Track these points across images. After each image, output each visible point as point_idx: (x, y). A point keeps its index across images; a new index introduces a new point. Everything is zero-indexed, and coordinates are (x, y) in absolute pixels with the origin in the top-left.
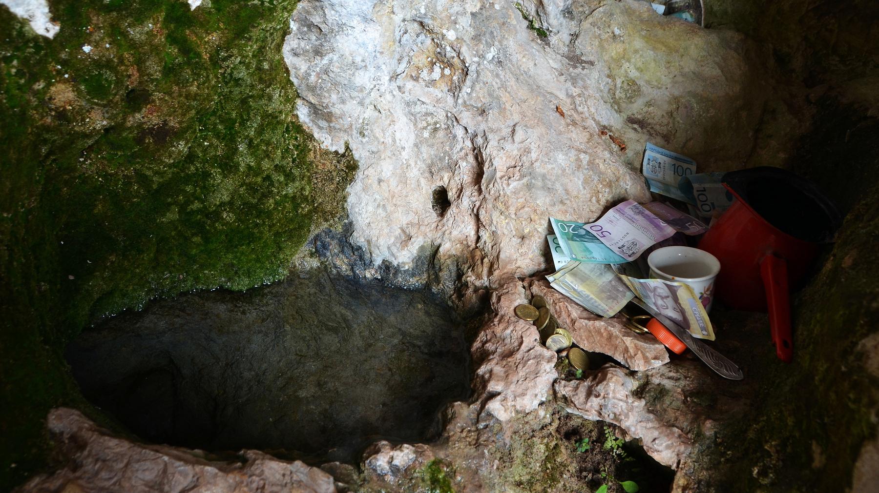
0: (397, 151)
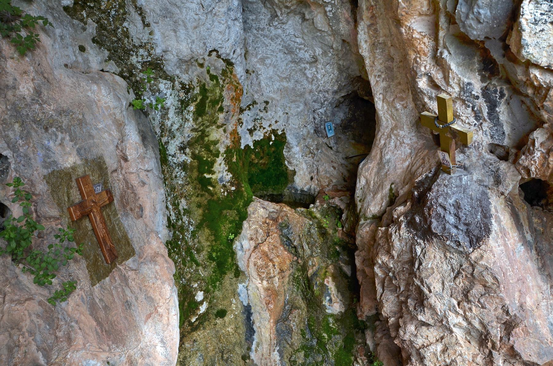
0: (303, 169)
